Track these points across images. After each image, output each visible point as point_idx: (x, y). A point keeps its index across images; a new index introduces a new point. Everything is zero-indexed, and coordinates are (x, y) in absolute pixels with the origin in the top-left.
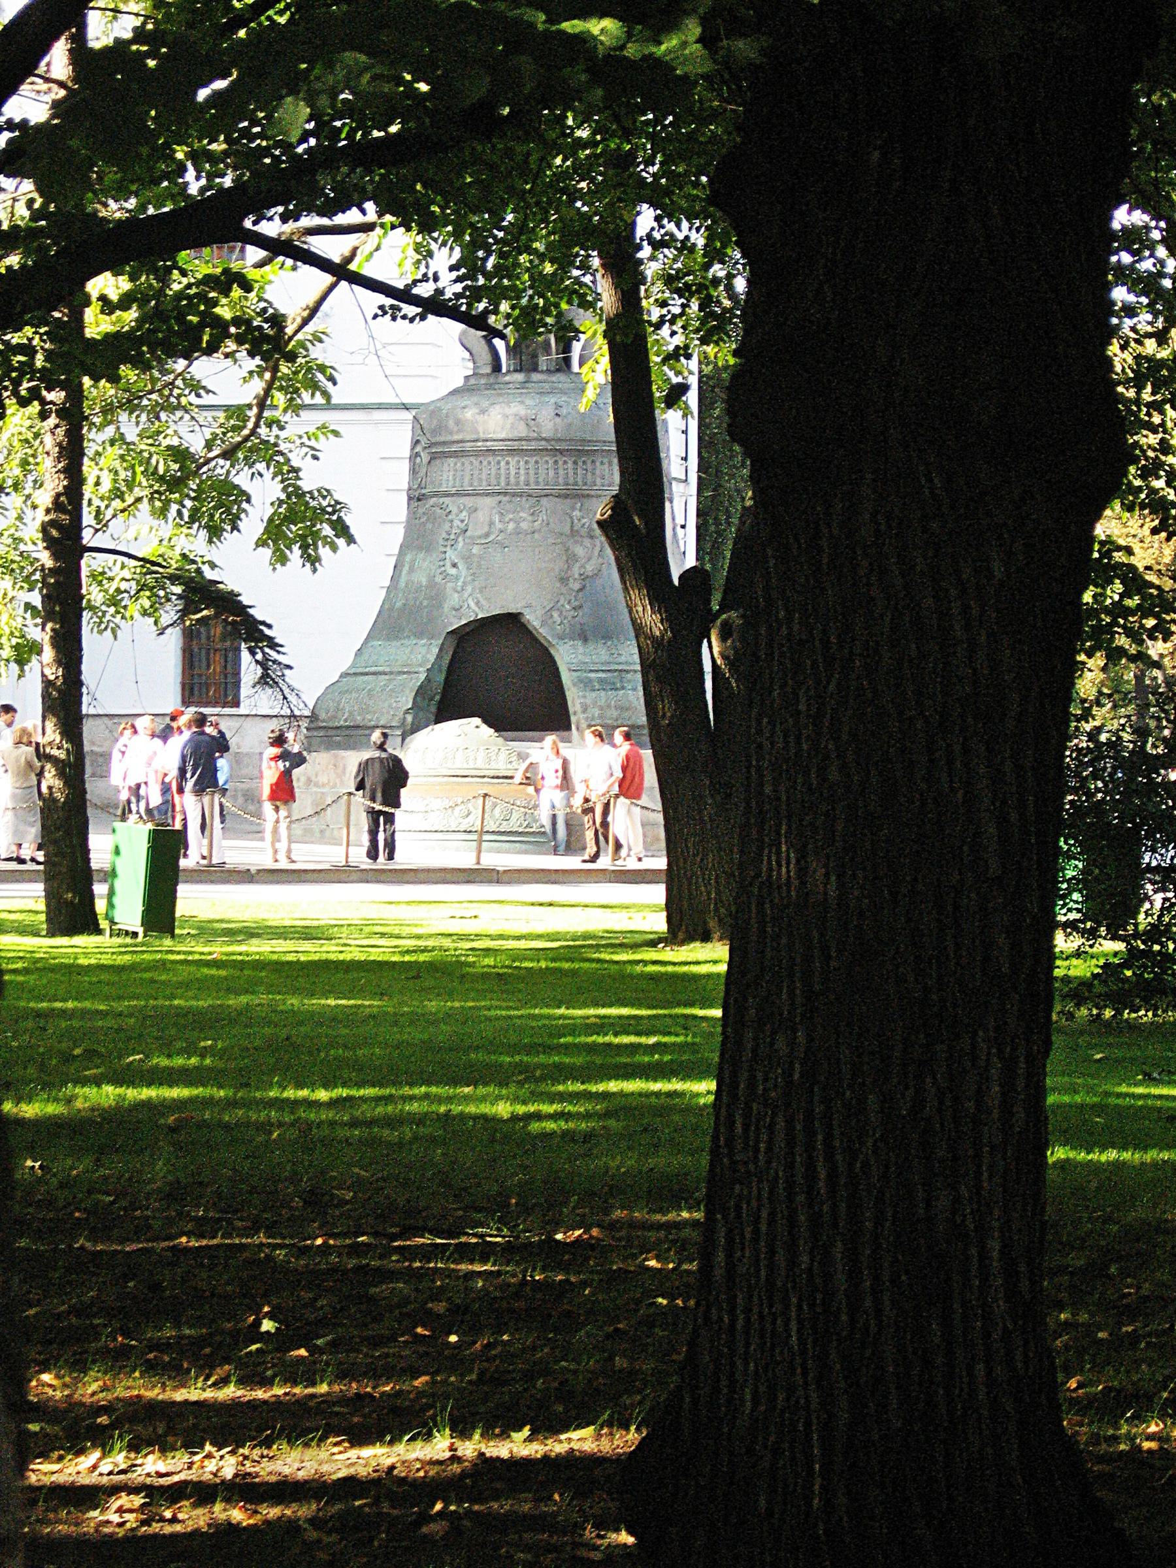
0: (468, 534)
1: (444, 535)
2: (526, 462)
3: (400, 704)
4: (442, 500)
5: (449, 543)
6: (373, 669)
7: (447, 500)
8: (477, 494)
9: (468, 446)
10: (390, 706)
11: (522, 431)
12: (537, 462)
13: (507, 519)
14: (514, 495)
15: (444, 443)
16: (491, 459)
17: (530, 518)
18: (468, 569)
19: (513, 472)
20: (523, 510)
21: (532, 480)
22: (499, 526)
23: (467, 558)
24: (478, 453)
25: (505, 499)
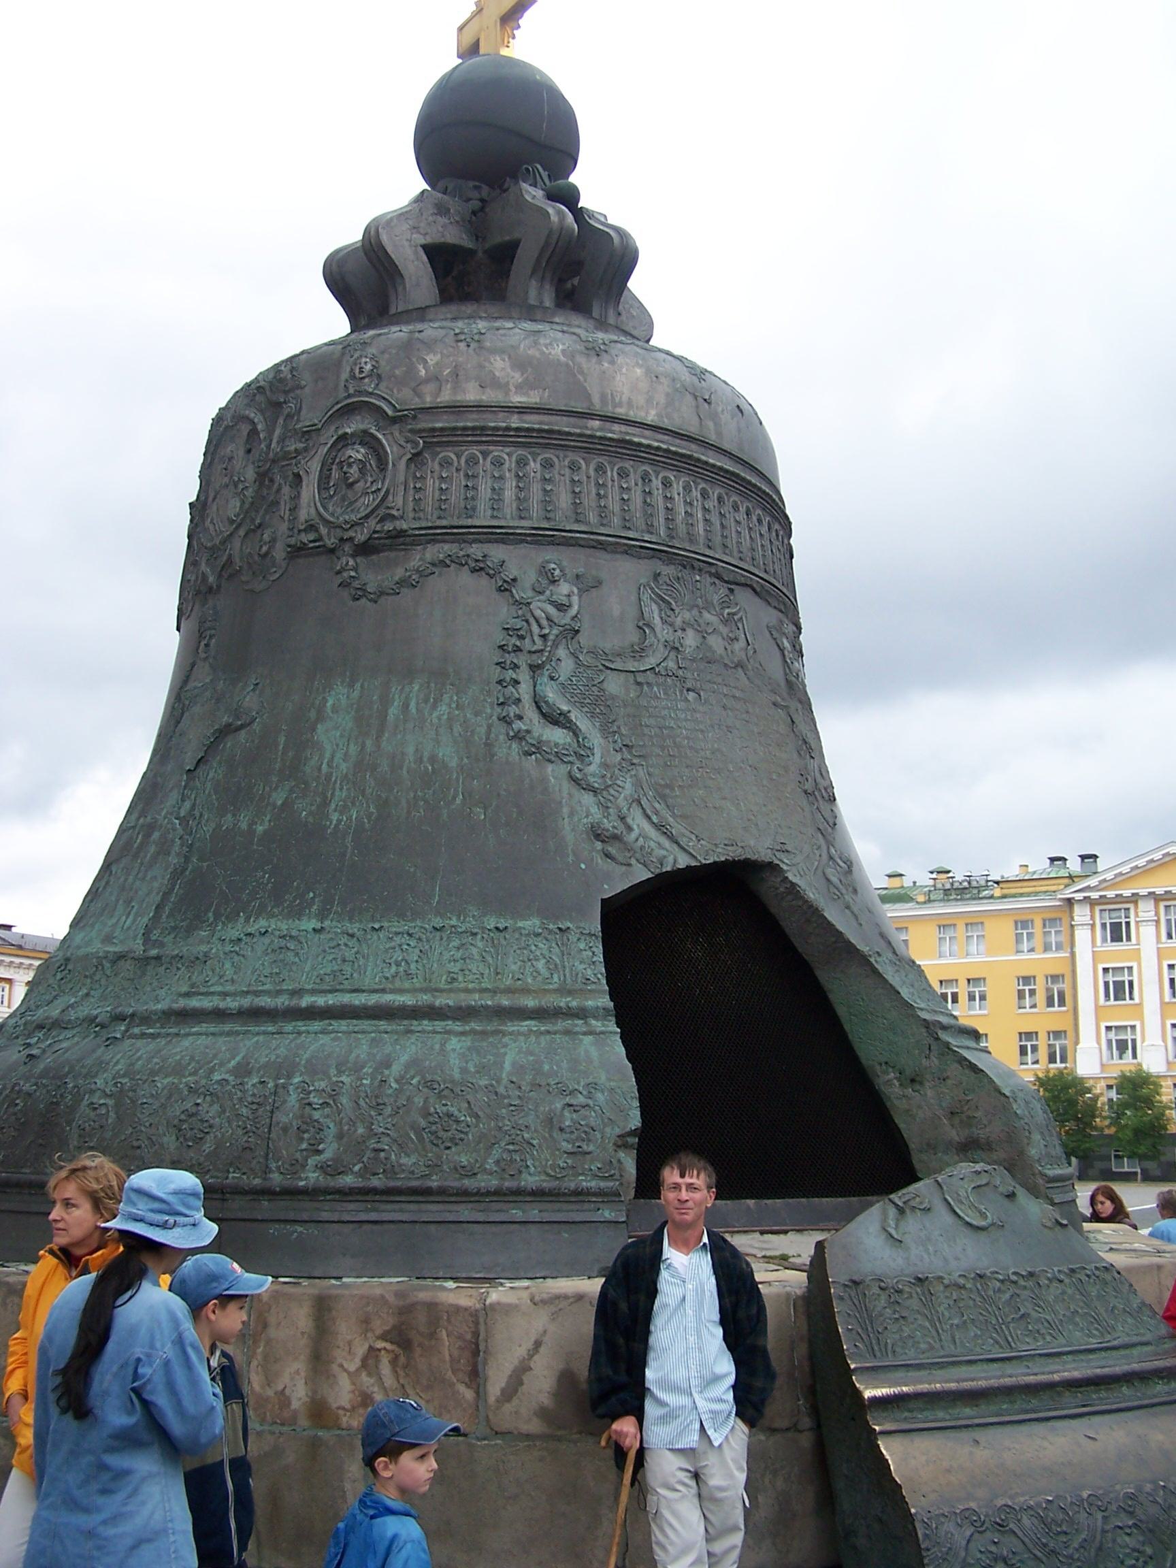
0: (583, 638)
1: (500, 638)
2: (705, 495)
3: (593, 1118)
4: (476, 550)
5: (522, 660)
6: (359, 1000)
7: (497, 553)
8: (601, 546)
9: (563, 424)
10: (550, 1121)
11: (685, 417)
12: (720, 499)
13: (679, 621)
14: (687, 564)
15: (480, 407)
16: (628, 465)
17: (724, 630)
18: (607, 729)
19: (681, 509)
20: (708, 606)
21: (718, 540)
22: (664, 633)
23: (599, 706)
24: (592, 445)
25: (668, 571)
